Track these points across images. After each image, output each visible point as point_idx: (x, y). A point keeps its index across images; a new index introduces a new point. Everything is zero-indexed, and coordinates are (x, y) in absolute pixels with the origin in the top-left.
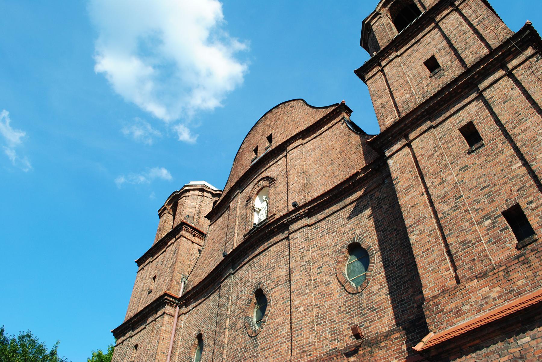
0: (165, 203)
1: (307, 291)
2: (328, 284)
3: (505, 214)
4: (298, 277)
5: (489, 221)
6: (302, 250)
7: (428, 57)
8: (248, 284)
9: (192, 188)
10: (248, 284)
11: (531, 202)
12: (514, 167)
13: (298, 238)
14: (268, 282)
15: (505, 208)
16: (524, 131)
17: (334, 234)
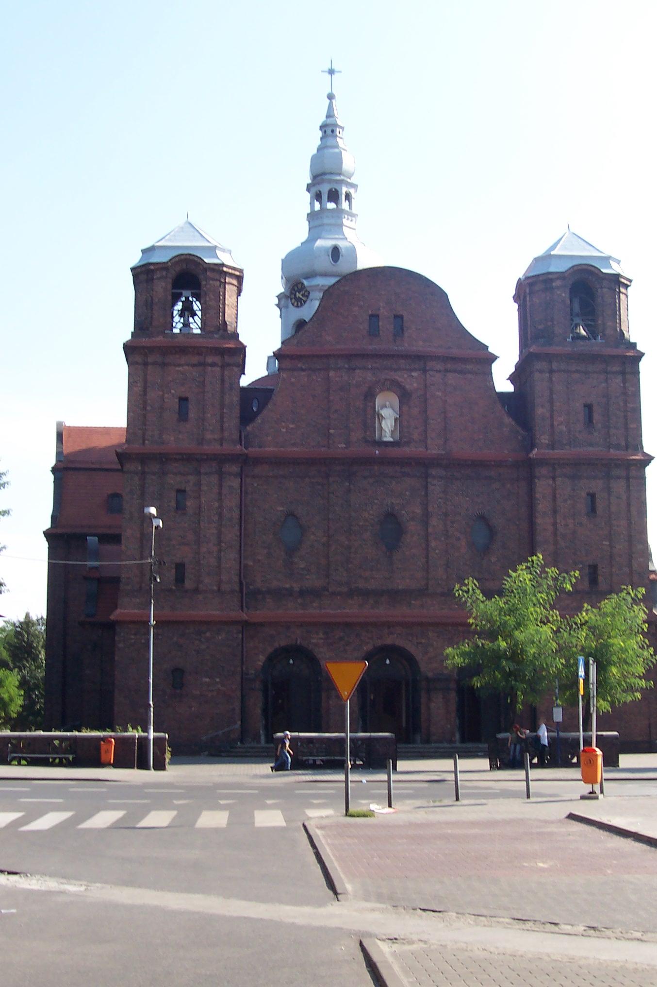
0: (170, 260)
1: (443, 539)
2: (458, 539)
3: (590, 566)
4: (435, 524)
5: (581, 566)
6: (440, 500)
7: (589, 402)
8: (376, 501)
9: (230, 271)
10: (376, 501)
11: (603, 568)
12: (605, 543)
13: (436, 487)
14: (403, 512)
15: (591, 563)
16: (618, 526)
17: (468, 499)
